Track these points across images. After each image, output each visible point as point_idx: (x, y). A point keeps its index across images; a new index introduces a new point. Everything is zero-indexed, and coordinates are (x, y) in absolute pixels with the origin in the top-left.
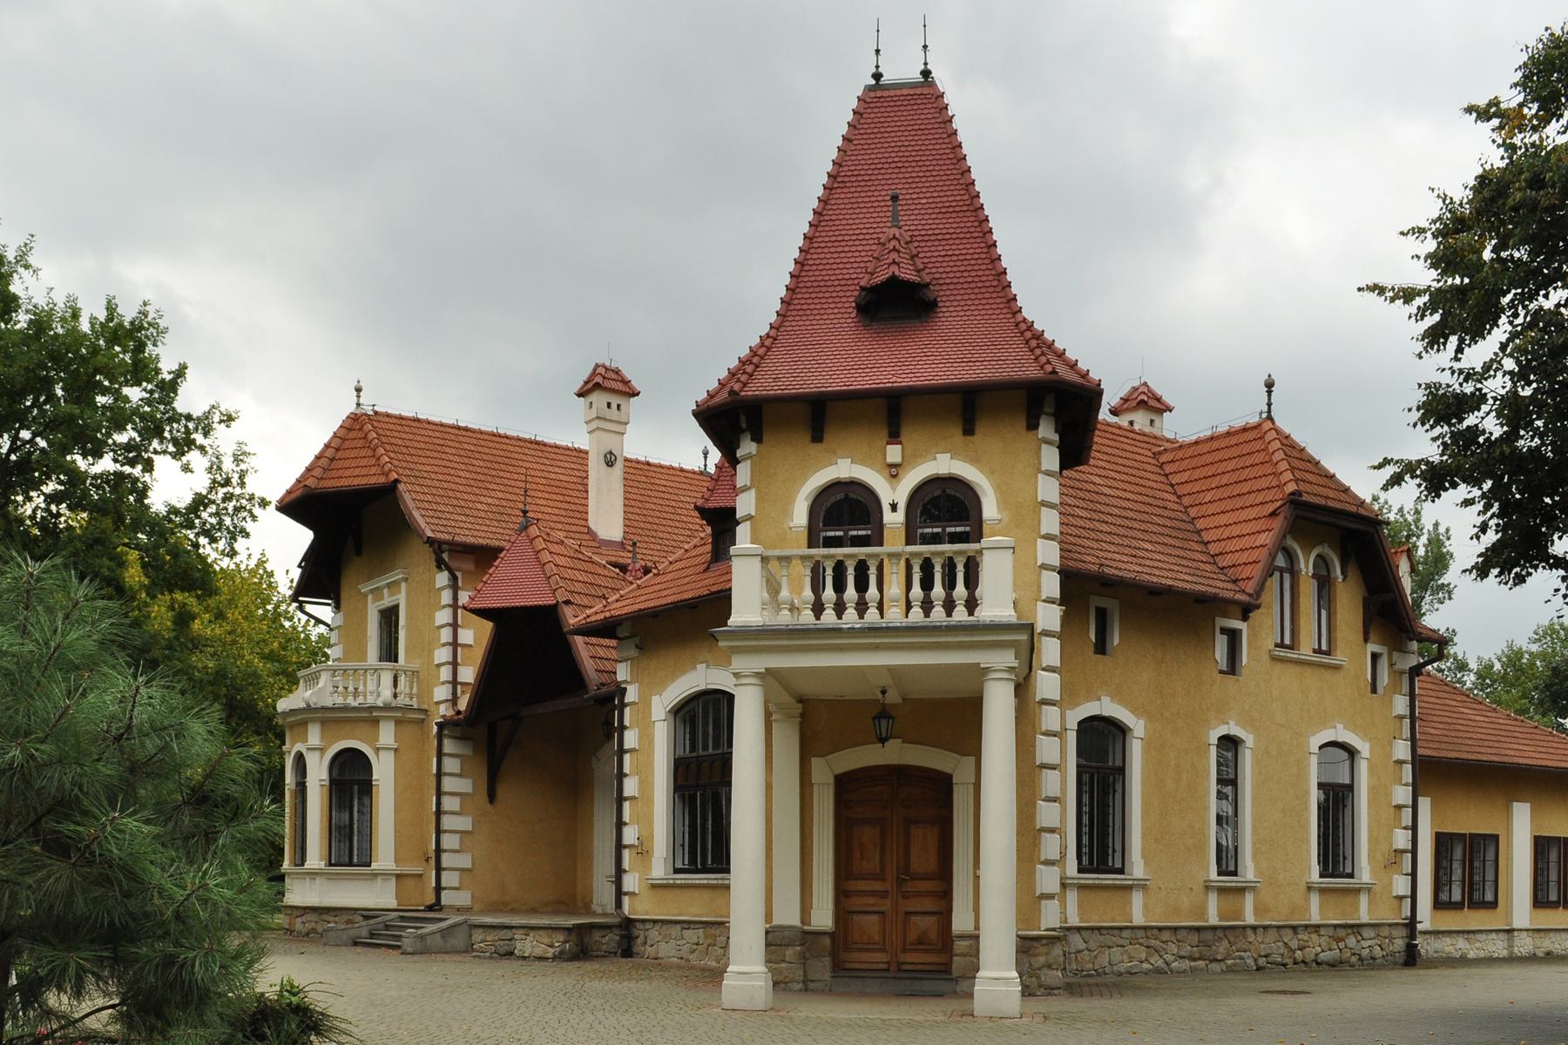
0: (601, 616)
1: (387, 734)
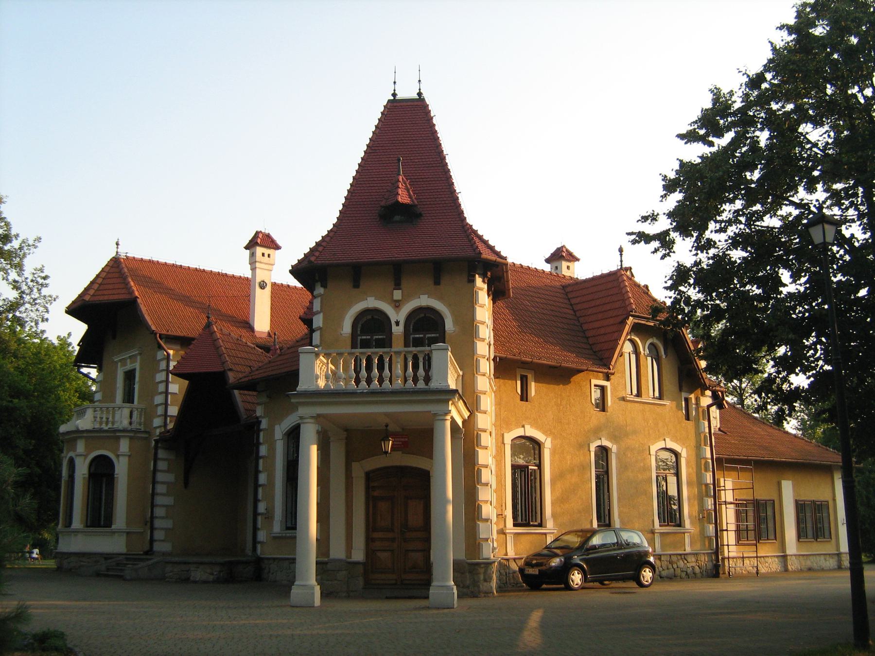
0: (246, 379)
1: (124, 446)
